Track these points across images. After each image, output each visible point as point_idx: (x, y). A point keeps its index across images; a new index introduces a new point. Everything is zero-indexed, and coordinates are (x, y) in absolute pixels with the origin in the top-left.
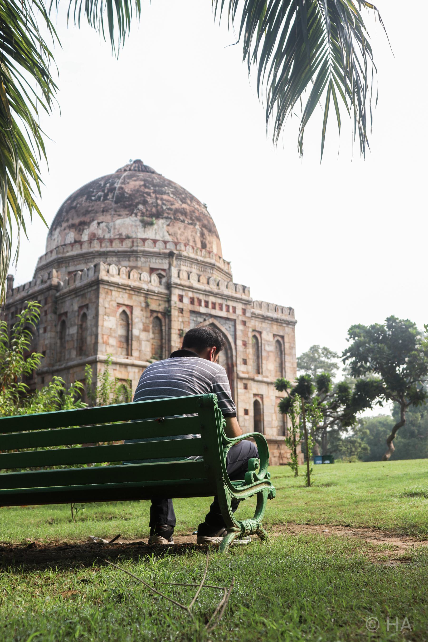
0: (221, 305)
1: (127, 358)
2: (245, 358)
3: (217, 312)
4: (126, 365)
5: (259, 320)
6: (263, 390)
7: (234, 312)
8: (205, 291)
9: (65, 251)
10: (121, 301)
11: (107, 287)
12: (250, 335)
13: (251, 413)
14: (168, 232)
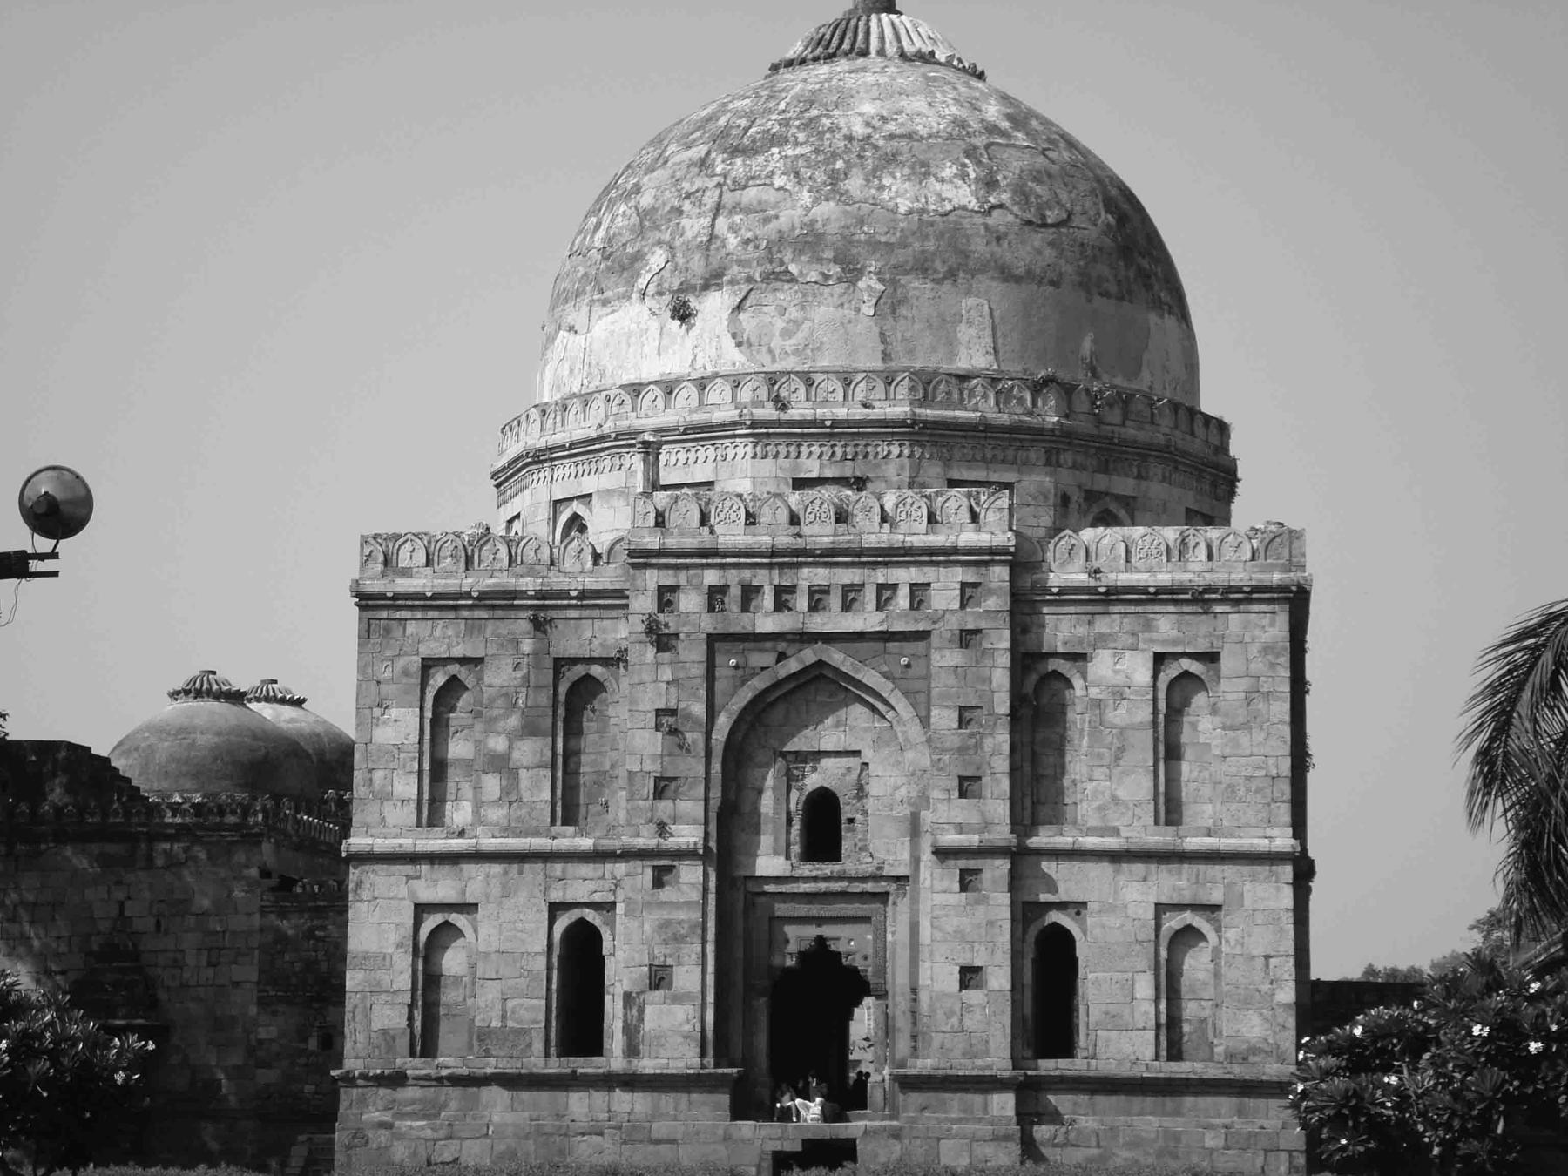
3: (833, 620)
5: (1080, 609)
8: (773, 553)
10: (439, 650)
11: (384, 614)
14: (734, 336)
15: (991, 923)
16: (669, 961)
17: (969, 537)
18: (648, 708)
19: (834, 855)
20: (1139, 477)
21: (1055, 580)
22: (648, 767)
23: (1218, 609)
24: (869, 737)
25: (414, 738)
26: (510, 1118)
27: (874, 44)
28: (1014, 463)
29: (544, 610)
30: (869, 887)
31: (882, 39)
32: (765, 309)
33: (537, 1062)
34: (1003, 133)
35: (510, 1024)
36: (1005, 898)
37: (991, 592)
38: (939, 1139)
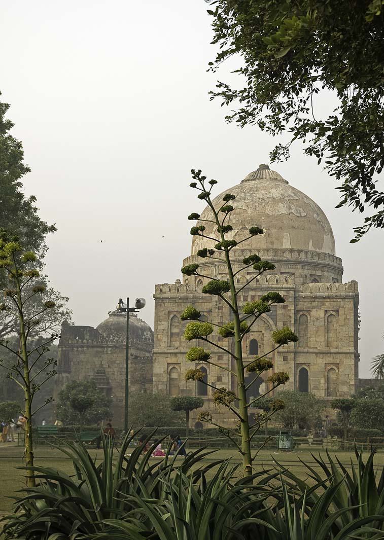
15: (290, 368)
17: (285, 285)
19: (257, 354)
20: (322, 271)
21: (303, 294)
22: (216, 334)
23: (339, 300)
24: (264, 328)
25: (167, 328)
27: (264, 176)
28: (295, 268)
31: (266, 175)
34: (292, 197)
35: (188, 388)
36: (293, 362)
37: (290, 297)
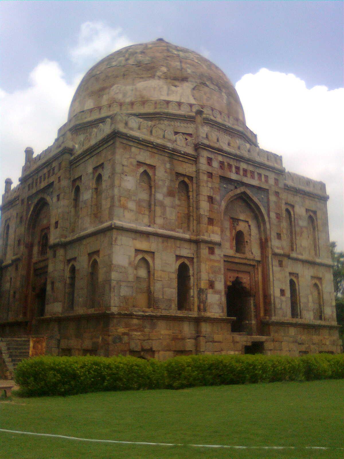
0: (252, 173)
1: (149, 226)
2: (279, 232)
4: (148, 235)
6: (299, 269)
7: (267, 181)
8: (236, 155)
9: (83, 117)
11: (125, 141)
12: (284, 207)
13: (288, 294)
14: (193, 96)
16: (214, 279)
18: (206, 195)
26: (167, 332)
29: (173, 155)
30: (252, 263)
32: (201, 92)
33: (174, 311)
35: (165, 297)
38: (282, 342)
